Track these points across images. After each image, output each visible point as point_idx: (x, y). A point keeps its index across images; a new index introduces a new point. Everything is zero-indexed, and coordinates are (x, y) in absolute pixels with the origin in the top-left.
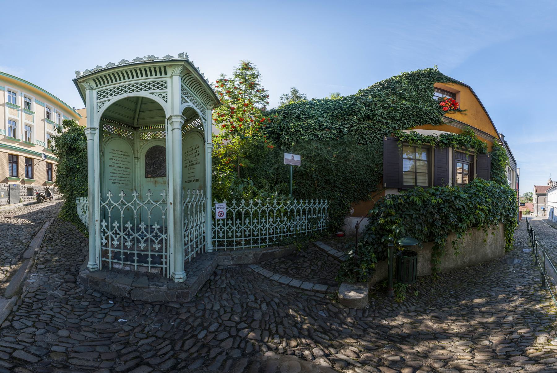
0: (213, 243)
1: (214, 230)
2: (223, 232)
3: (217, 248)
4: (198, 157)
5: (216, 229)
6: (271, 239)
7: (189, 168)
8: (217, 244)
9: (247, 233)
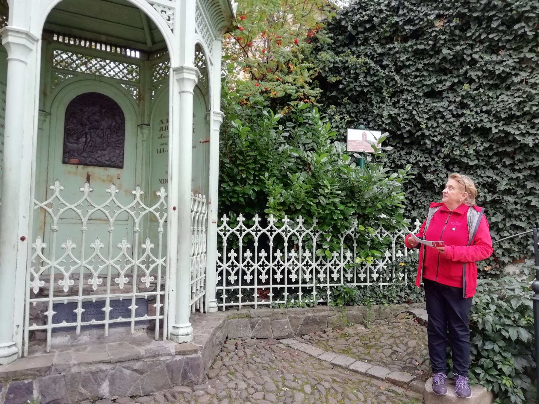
0: (218, 294)
1: (220, 269)
2: (237, 274)
3: (224, 304)
5: (225, 266)
6: (322, 291)
8: (224, 296)
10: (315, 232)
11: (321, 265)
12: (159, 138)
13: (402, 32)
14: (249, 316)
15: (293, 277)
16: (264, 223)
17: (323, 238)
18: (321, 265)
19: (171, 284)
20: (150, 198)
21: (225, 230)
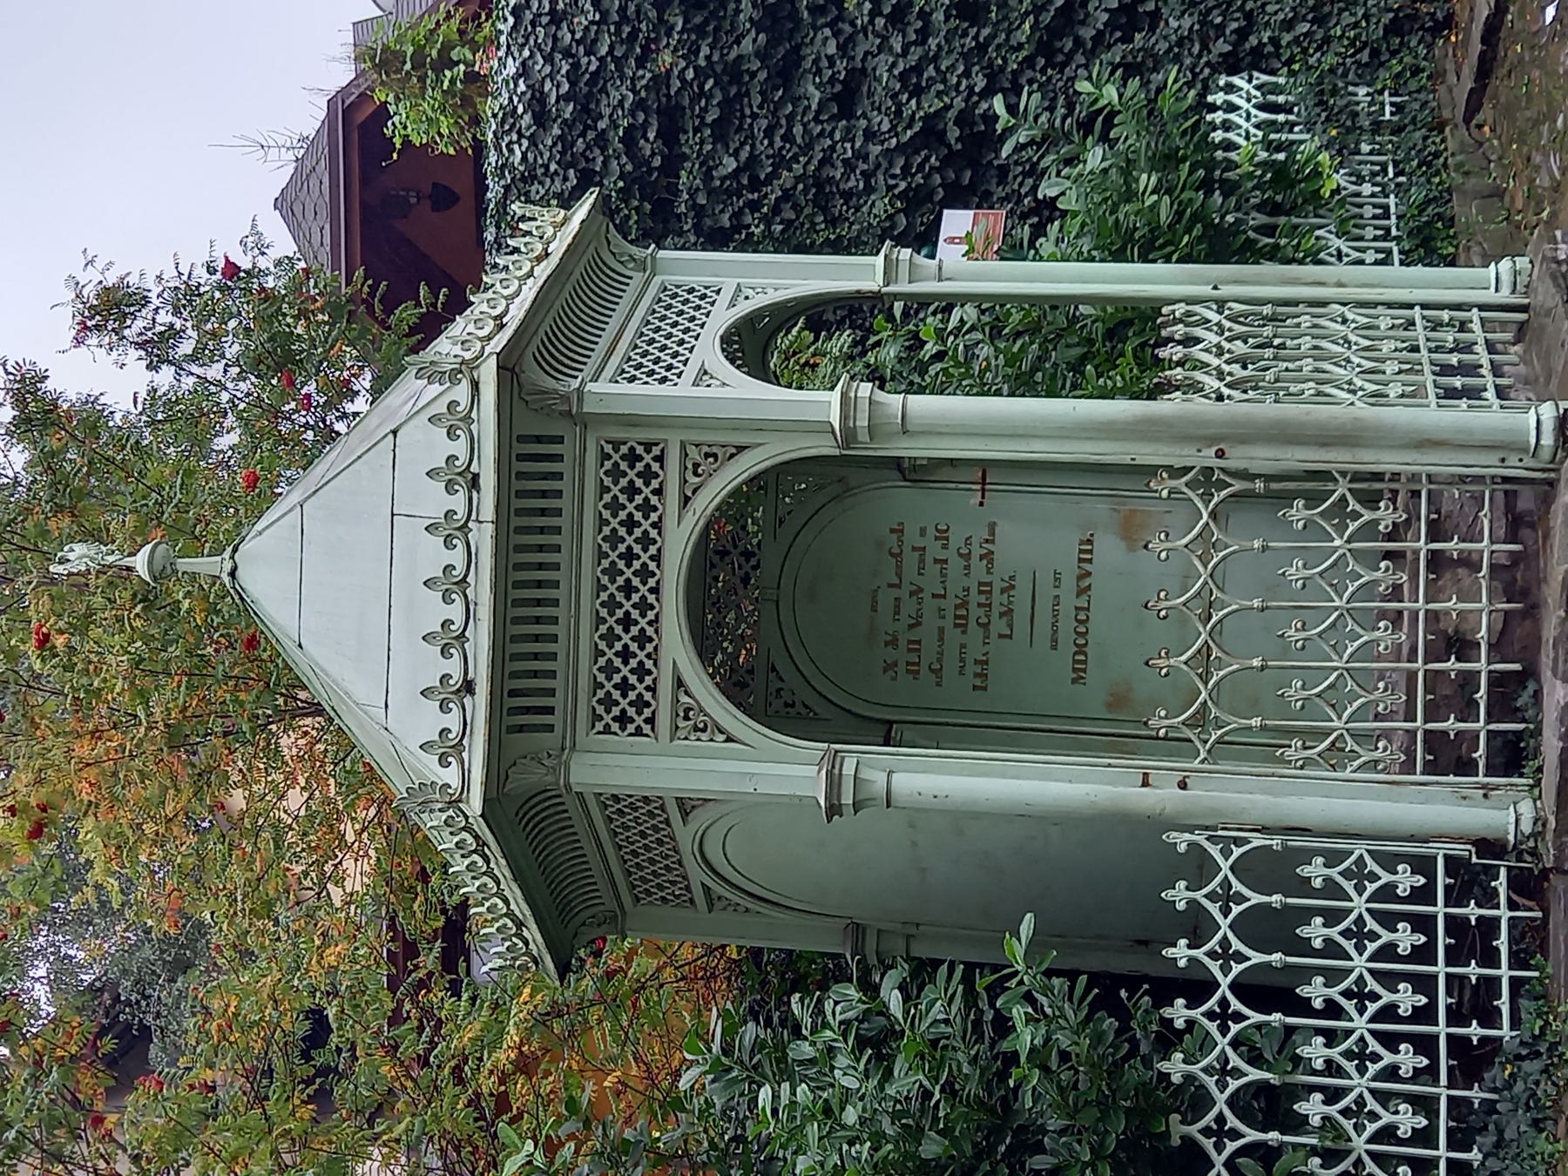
4: (956, 540)
7: (999, 626)
12: (938, 684)
13: (651, 170)
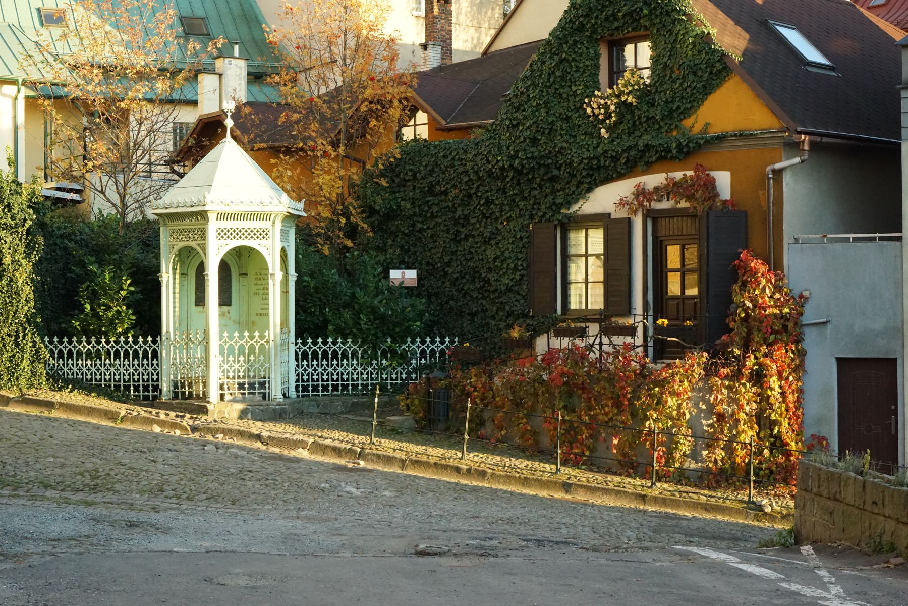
0: (297, 387)
5: (300, 370)
8: (300, 389)
9: (335, 377)
10: (359, 347)
11: (365, 369)
14: (315, 400)
15: (345, 377)
16: (325, 343)
17: (365, 352)
18: (365, 369)
19: (272, 376)
20: (262, 337)
21: (299, 348)
